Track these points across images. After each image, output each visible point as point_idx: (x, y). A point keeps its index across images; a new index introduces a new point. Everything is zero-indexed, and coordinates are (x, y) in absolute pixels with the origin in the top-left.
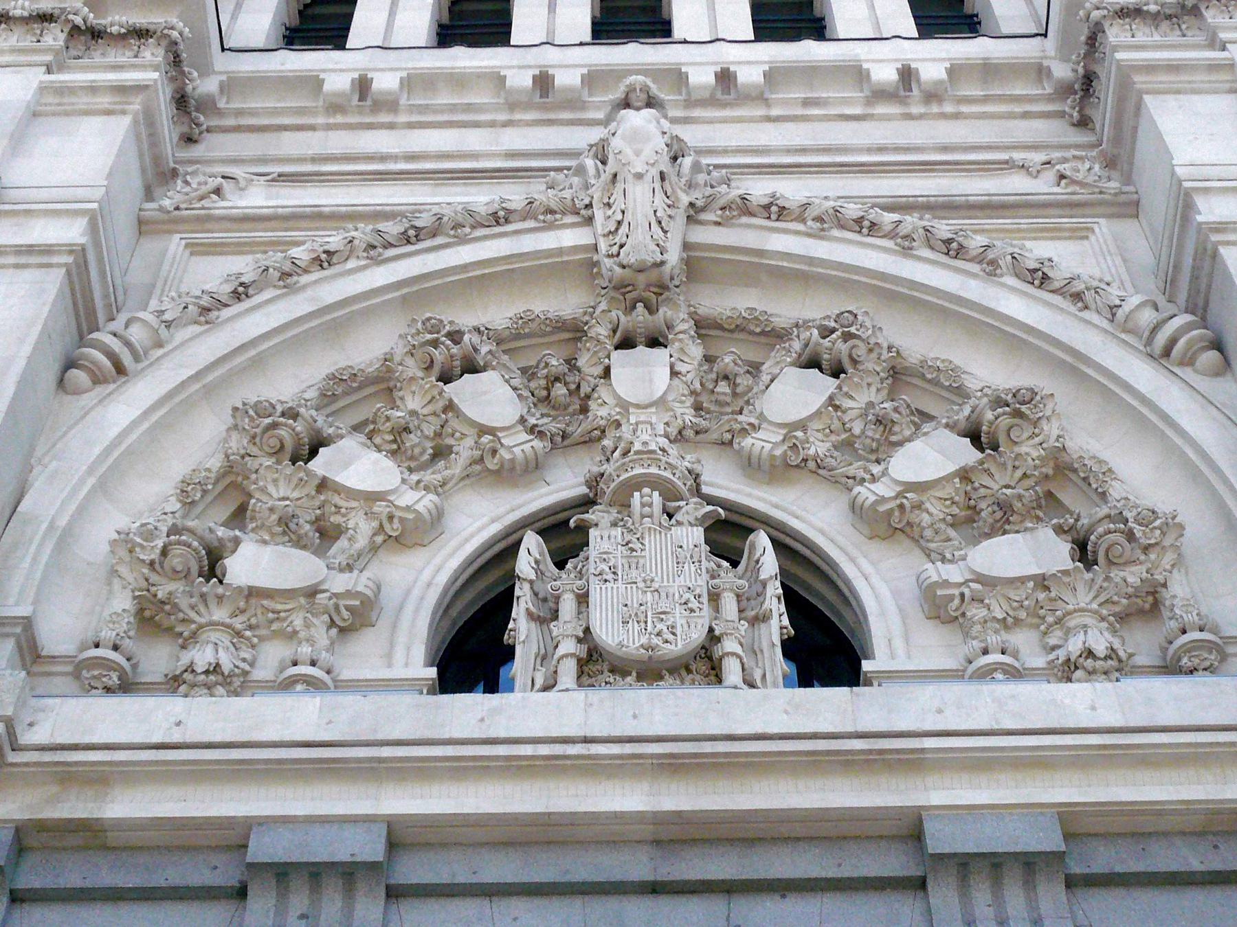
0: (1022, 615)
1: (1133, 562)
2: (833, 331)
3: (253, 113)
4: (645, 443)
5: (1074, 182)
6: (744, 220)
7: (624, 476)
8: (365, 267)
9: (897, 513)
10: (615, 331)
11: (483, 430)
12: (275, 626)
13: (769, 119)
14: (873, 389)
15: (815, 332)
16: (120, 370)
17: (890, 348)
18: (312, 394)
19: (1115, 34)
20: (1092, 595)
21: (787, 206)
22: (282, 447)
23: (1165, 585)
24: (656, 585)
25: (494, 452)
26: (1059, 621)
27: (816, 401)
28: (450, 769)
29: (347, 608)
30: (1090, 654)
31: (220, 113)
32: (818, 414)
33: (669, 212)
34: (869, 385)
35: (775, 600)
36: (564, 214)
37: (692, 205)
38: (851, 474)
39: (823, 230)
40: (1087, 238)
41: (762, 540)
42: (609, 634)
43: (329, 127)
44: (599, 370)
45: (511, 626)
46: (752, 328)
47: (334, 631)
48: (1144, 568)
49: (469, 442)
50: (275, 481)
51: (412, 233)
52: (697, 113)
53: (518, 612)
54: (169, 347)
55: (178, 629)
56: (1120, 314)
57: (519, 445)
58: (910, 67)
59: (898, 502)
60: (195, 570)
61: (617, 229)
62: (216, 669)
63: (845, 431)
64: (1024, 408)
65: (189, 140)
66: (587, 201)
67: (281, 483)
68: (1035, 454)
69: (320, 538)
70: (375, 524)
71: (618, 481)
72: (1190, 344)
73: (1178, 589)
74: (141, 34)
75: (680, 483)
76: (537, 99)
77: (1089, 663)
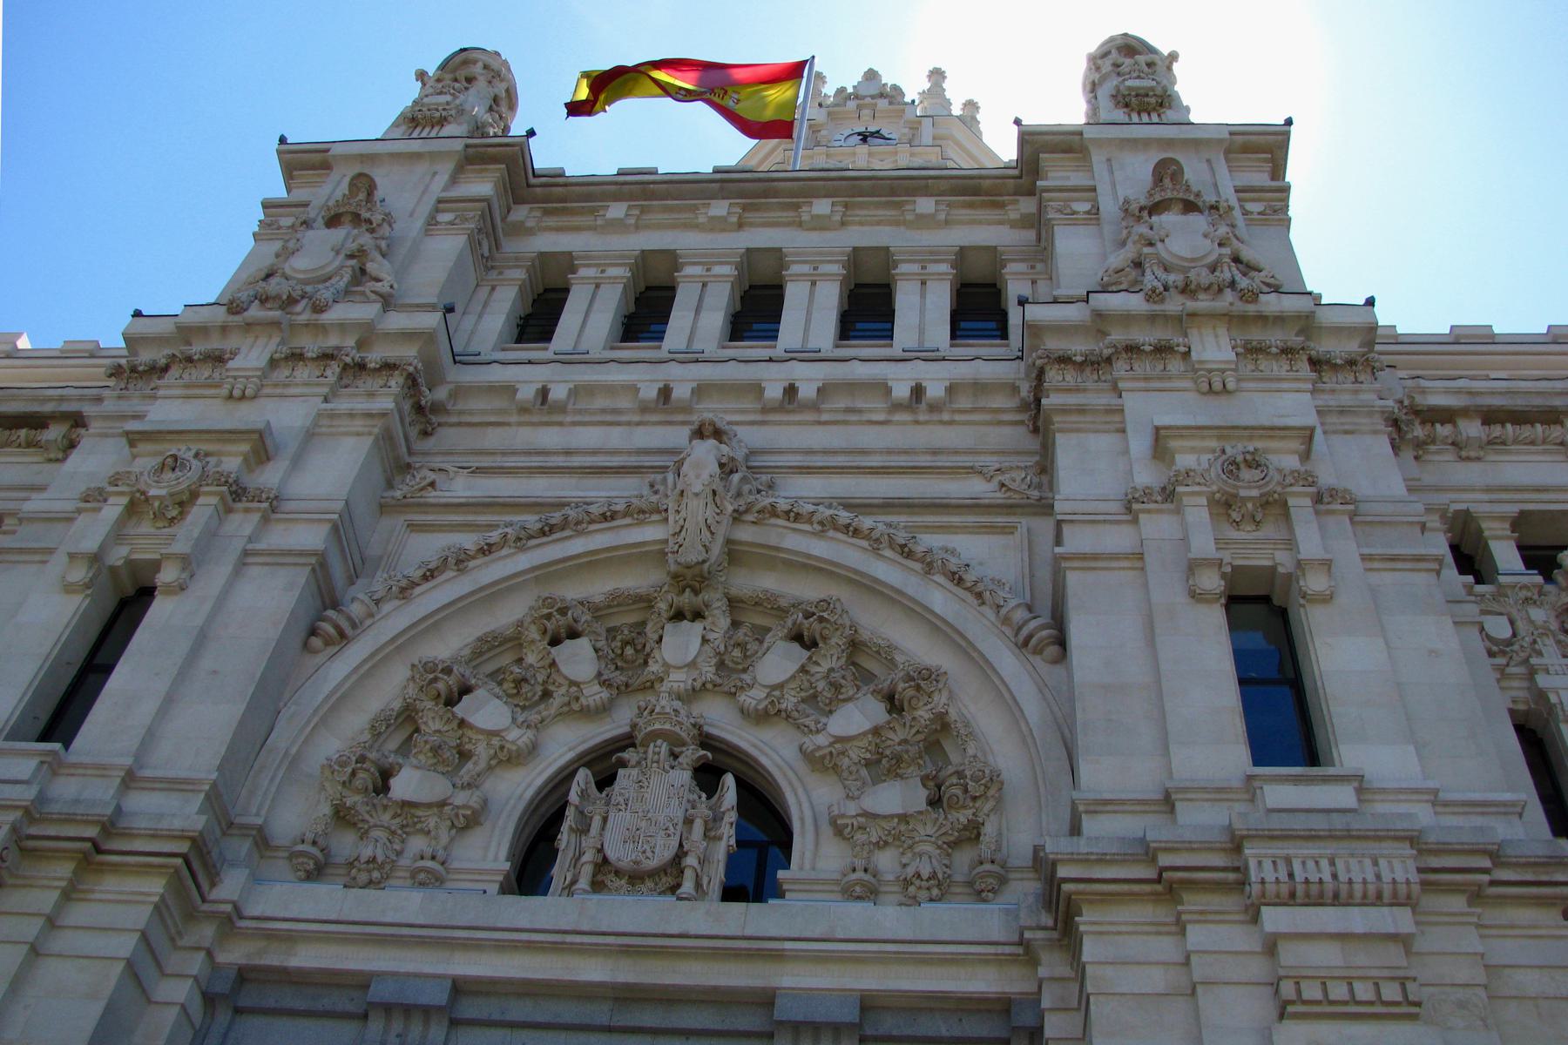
0: (890, 840)
1: (964, 807)
2: (814, 614)
3: (471, 413)
4: (663, 707)
6: (773, 521)
7: (649, 729)
8: (513, 554)
9: (828, 757)
10: (671, 607)
11: (573, 683)
12: (419, 826)
13: (819, 423)
14: (835, 658)
15: (801, 615)
16: (342, 635)
17: (851, 627)
18: (467, 652)
19: (1053, 376)
20: (936, 828)
21: (800, 512)
22: (439, 695)
23: (983, 824)
24: (650, 815)
25: (577, 699)
26: (910, 847)
27: (792, 668)
28: (495, 946)
29: (464, 816)
30: (918, 876)
31: (447, 412)
32: (793, 677)
33: (717, 518)
34: (832, 655)
35: (728, 826)
36: (651, 513)
37: (735, 511)
38: (807, 723)
39: (823, 531)
40: (1013, 533)
41: (729, 780)
42: (611, 854)
43: (520, 424)
44: (656, 637)
45: (559, 837)
46: (765, 604)
47: (453, 832)
48: (971, 811)
49: (563, 690)
50: (433, 718)
51: (547, 529)
52: (771, 417)
53: (565, 827)
54: (377, 617)
55: (360, 825)
56: (1003, 611)
57: (594, 694)
58: (921, 384)
59: (830, 749)
60: (371, 787)
61: (680, 531)
63: (811, 688)
64: (922, 683)
65: (425, 434)
66: (665, 507)
67: (437, 720)
68: (927, 716)
69: (459, 758)
70: (492, 752)
71: (645, 731)
72: (1041, 640)
73: (989, 829)
74: (389, 367)
75: (684, 735)
76: (661, 406)
77: (918, 882)
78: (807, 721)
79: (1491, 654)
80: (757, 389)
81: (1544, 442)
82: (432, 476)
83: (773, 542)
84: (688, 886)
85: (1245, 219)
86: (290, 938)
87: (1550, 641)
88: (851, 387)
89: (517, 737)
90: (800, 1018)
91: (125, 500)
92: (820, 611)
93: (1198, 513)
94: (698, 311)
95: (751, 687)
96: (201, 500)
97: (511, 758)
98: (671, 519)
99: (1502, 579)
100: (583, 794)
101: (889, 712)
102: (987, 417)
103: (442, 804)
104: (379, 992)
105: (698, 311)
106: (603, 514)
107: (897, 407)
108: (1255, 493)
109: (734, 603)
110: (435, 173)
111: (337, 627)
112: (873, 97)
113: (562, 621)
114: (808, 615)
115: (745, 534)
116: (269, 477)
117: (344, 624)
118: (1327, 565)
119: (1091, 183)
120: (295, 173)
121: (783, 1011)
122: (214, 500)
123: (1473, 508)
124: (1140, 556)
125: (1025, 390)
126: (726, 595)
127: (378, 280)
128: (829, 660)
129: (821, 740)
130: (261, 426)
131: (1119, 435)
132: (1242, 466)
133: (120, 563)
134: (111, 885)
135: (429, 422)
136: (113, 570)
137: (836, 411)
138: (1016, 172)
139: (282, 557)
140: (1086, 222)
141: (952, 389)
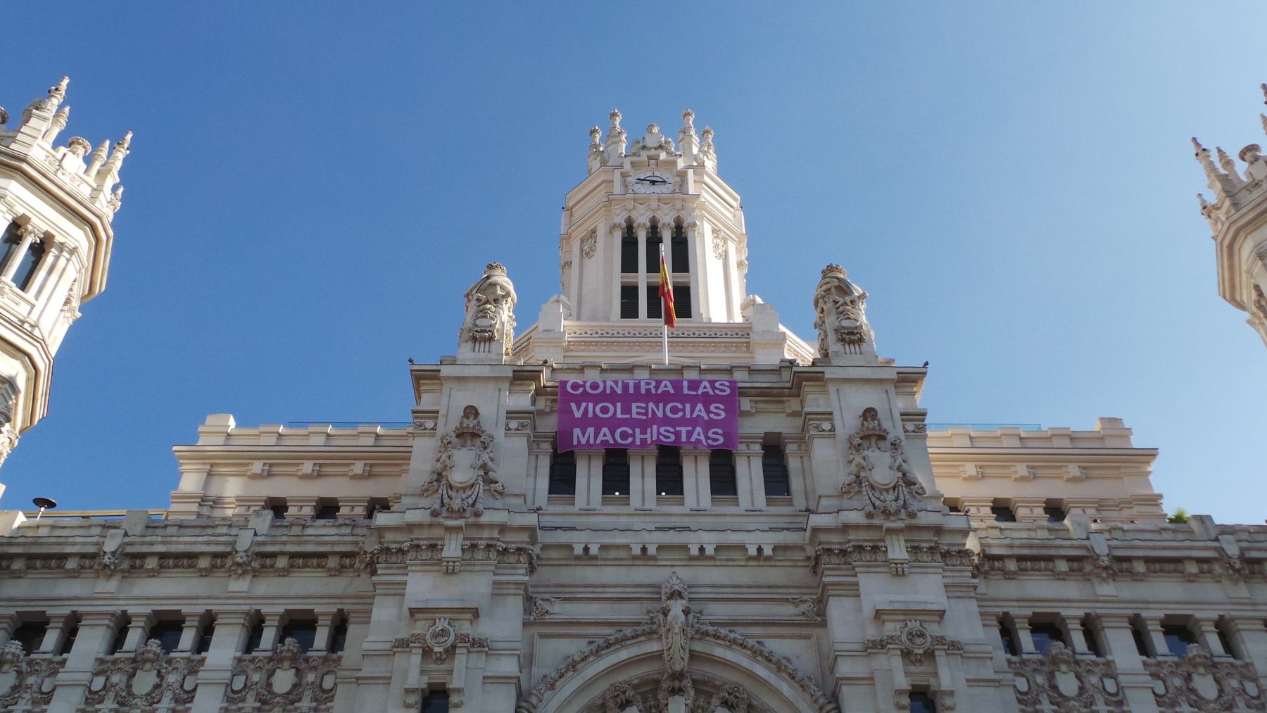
5: (807, 616)
6: (707, 638)
19: (824, 559)
44: (665, 702)
79: (1018, 699)
81: (1046, 570)
82: (546, 606)
85: (905, 435)
87: (1045, 696)
91: (420, 651)
92: (735, 690)
93: (897, 662)
96: (458, 651)
98: (664, 640)
99: (1023, 655)
102: (791, 563)
106: (633, 636)
107: (751, 558)
108: (921, 651)
109: (695, 682)
112: (656, 149)
115: (699, 647)
118: (952, 693)
119: (829, 410)
120: (421, 382)
122: (465, 651)
123: (1013, 612)
124: (872, 679)
125: (810, 552)
126: (691, 678)
131: (856, 598)
132: (916, 636)
135: (534, 567)
136: (423, 690)
137: (721, 560)
138: (787, 385)
140: (829, 437)
141: (776, 548)
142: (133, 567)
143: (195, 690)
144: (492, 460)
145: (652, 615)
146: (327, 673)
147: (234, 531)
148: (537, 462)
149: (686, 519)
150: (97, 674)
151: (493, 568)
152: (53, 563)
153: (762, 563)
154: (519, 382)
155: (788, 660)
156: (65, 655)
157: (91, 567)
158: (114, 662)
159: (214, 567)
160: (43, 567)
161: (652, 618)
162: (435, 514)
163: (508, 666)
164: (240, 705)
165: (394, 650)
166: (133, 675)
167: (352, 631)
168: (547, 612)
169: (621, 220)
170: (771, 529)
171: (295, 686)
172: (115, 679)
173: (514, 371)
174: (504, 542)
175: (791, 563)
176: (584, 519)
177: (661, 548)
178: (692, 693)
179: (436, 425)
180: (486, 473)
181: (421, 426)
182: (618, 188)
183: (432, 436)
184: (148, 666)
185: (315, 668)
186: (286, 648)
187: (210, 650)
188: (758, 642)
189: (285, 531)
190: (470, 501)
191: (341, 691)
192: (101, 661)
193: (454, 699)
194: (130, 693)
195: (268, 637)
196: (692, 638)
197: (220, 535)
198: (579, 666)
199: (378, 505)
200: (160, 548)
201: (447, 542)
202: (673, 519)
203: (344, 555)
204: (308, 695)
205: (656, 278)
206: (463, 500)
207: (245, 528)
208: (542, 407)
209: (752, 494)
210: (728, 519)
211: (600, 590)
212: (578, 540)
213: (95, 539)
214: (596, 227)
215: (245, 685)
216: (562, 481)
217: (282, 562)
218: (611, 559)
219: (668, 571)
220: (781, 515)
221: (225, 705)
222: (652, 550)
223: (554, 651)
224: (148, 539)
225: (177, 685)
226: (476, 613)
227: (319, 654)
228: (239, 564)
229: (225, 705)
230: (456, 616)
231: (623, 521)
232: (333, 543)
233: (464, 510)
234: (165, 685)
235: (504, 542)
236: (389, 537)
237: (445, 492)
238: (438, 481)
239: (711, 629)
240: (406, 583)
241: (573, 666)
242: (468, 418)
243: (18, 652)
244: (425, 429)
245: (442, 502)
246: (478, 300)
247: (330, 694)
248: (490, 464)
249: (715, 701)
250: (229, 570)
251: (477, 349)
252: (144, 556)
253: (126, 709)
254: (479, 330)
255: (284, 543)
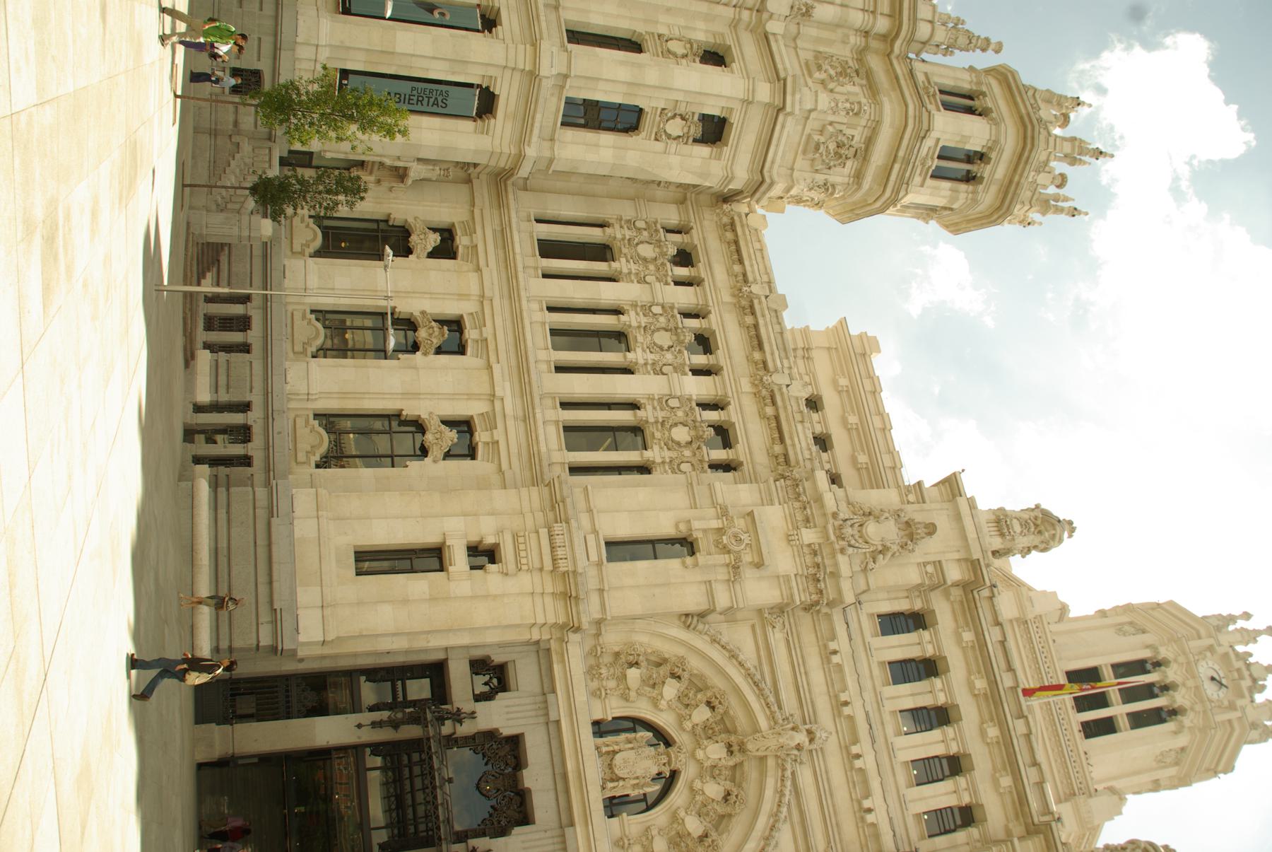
3: (820, 625)
6: (780, 771)
11: (690, 716)
13: (846, 772)
16: (689, 626)
18: (695, 672)
42: (618, 756)
43: (819, 646)
52: (844, 751)
62: (601, 674)
78: (692, 807)
80: (856, 741)
82: (778, 626)
83: (769, 774)
84: (610, 785)
86: (563, 661)
88: (865, 782)
89: (663, 704)
90: (566, 836)
91: (721, 526)
94: (912, 695)
95: (702, 782)
96: (727, 556)
97: (655, 703)
100: (642, 737)
101: (699, 837)
102: (863, 842)
103: (629, 689)
104: (550, 697)
105: (912, 695)
107: (860, 803)
109: (741, 763)
110: (959, 551)
111: (691, 623)
113: (716, 703)
114: (737, 796)
115: (771, 762)
116: (748, 573)
117: (692, 627)
120: (947, 484)
121: (568, 831)
122: (728, 561)
127: (874, 562)
128: (721, 809)
129: (682, 814)
130: (766, 563)
133: (695, 536)
134: (560, 605)
135: (809, 610)
136: (691, 535)
139: (711, 595)
141: (873, 825)
142: (744, 308)
143: (663, 374)
144: (893, 555)
145: (790, 718)
146: (692, 465)
147: (786, 371)
148: (903, 598)
149: (882, 740)
150: (663, 307)
151: (800, 573)
152: (736, 257)
153: (857, 815)
154: (970, 567)
155: (777, 845)
156: (672, 283)
157: (738, 282)
158: (673, 316)
159: (756, 363)
160: (731, 251)
161: (788, 719)
162: (835, 515)
163: (723, 600)
164: (658, 408)
165: (718, 507)
166: (667, 330)
167: (730, 475)
168: (774, 627)
169: (1164, 653)
170: (891, 819)
171: (678, 444)
172: (662, 319)
173: (978, 560)
174: (824, 578)
175: (863, 842)
176: (861, 648)
177: (851, 718)
178: (731, 763)
179: (913, 503)
180: (880, 552)
181: (908, 491)
182: (1195, 644)
183: (903, 503)
184: (674, 338)
185: (694, 455)
186: (705, 429)
187: (694, 377)
188: (786, 817)
189: (795, 408)
190: (853, 542)
191: (681, 477)
192: (672, 308)
193: (689, 560)
194: (653, 332)
195: (713, 416)
196: (777, 756)
197: (782, 362)
198: (734, 661)
199: (835, 479)
200: (761, 322)
201: (813, 530)
202: (880, 728)
203: (786, 456)
204: (673, 454)
205: (1114, 695)
206: (852, 536)
207: (791, 379)
208: (965, 639)
209: (921, 799)
210: (891, 779)
211: (802, 670)
212: (842, 643)
213: (758, 278)
214: (1149, 632)
215: (673, 408)
216: (893, 623)
217: (769, 411)
218: (830, 676)
219: (832, 729)
220: (907, 830)
221: (656, 397)
222: (847, 711)
223: (743, 638)
224: (766, 312)
225: (665, 361)
226: (759, 565)
227: (706, 456)
228: (761, 380)
229: (656, 397)
230: (754, 548)
231: (868, 684)
232: (794, 445)
233: (843, 539)
234: (663, 353)
235: (824, 578)
236: (807, 484)
237: (855, 521)
238: (864, 515)
239: (788, 773)
240: (772, 505)
241: (733, 656)
242: (925, 528)
243: (669, 253)
244: (907, 496)
245: (846, 520)
246: (1036, 518)
247: (677, 471)
248: (889, 554)
249: (728, 785)
250: (755, 375)
251: (990, 525)
252: (753, 313)
253: (642, 332)
254: (1008, 523)
255: (785, 408)
